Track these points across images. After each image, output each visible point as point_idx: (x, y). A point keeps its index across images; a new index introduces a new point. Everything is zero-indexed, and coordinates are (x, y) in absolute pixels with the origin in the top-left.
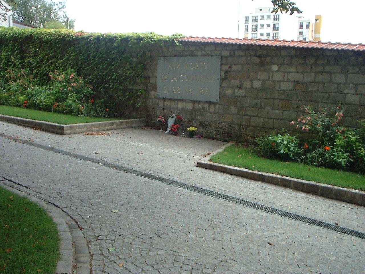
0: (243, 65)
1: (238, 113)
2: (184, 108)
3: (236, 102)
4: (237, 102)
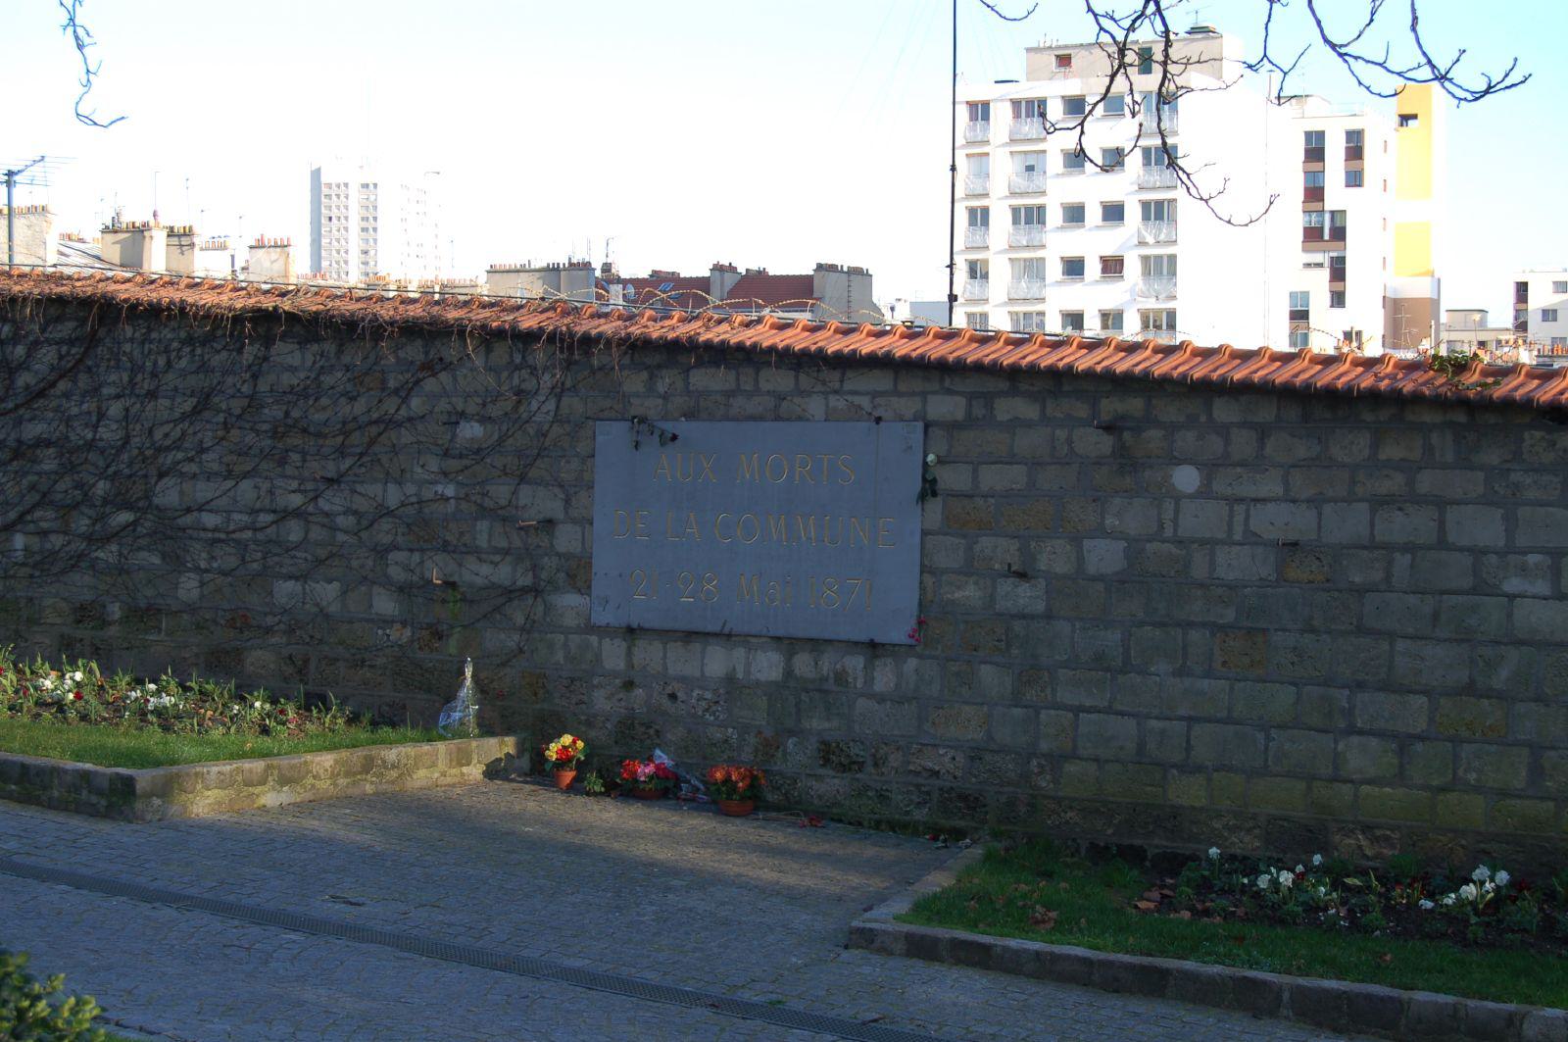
2: (740, 676)
3: (1003, 645)
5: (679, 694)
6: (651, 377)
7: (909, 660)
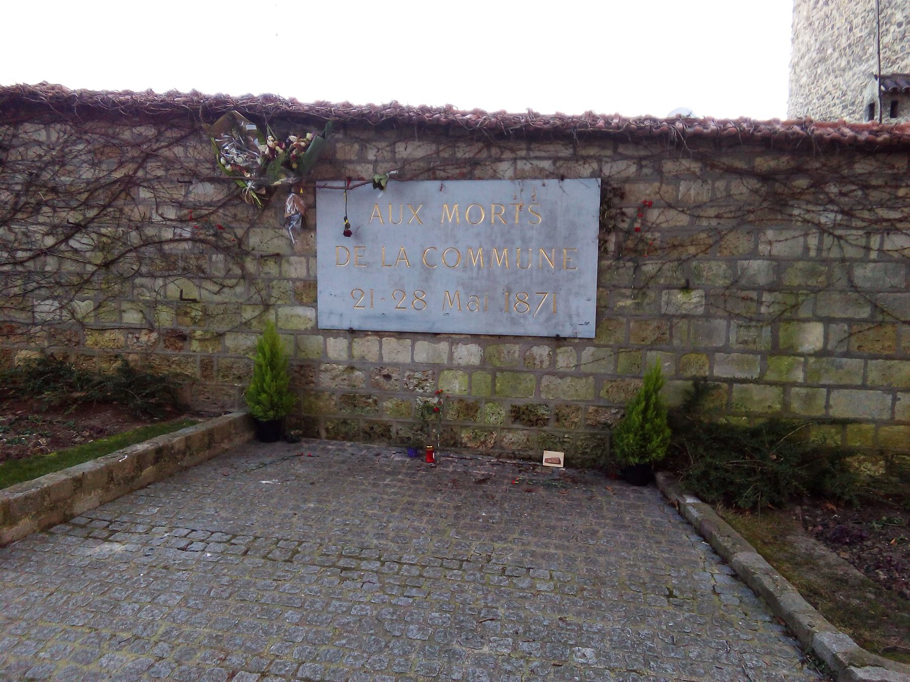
5: (393, 375)
7: (587, 348)
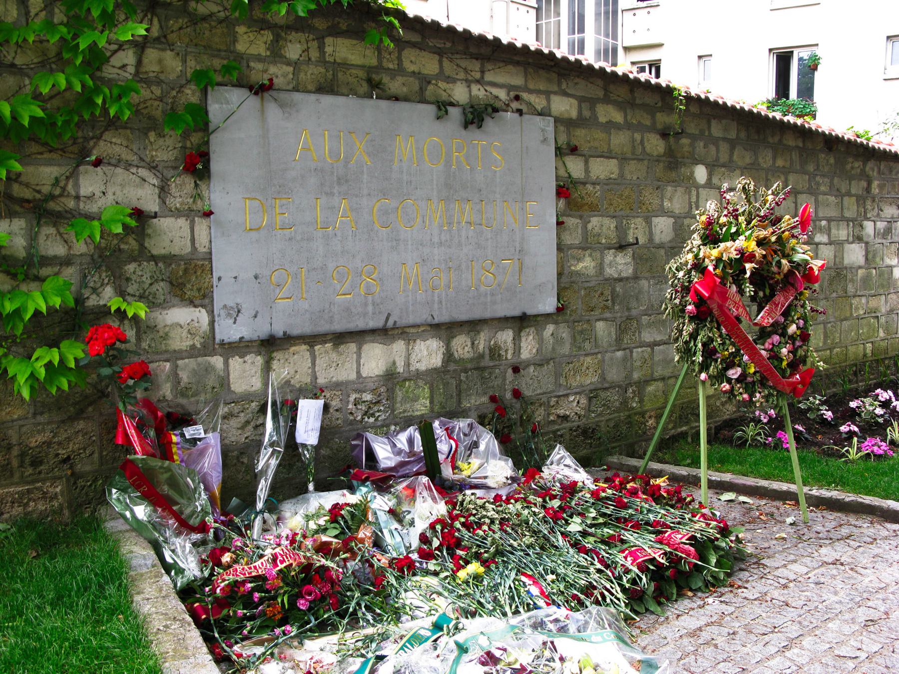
0: (623, 160)
1: (619, 344)
4: (613, 303)
6: (277, 39)
